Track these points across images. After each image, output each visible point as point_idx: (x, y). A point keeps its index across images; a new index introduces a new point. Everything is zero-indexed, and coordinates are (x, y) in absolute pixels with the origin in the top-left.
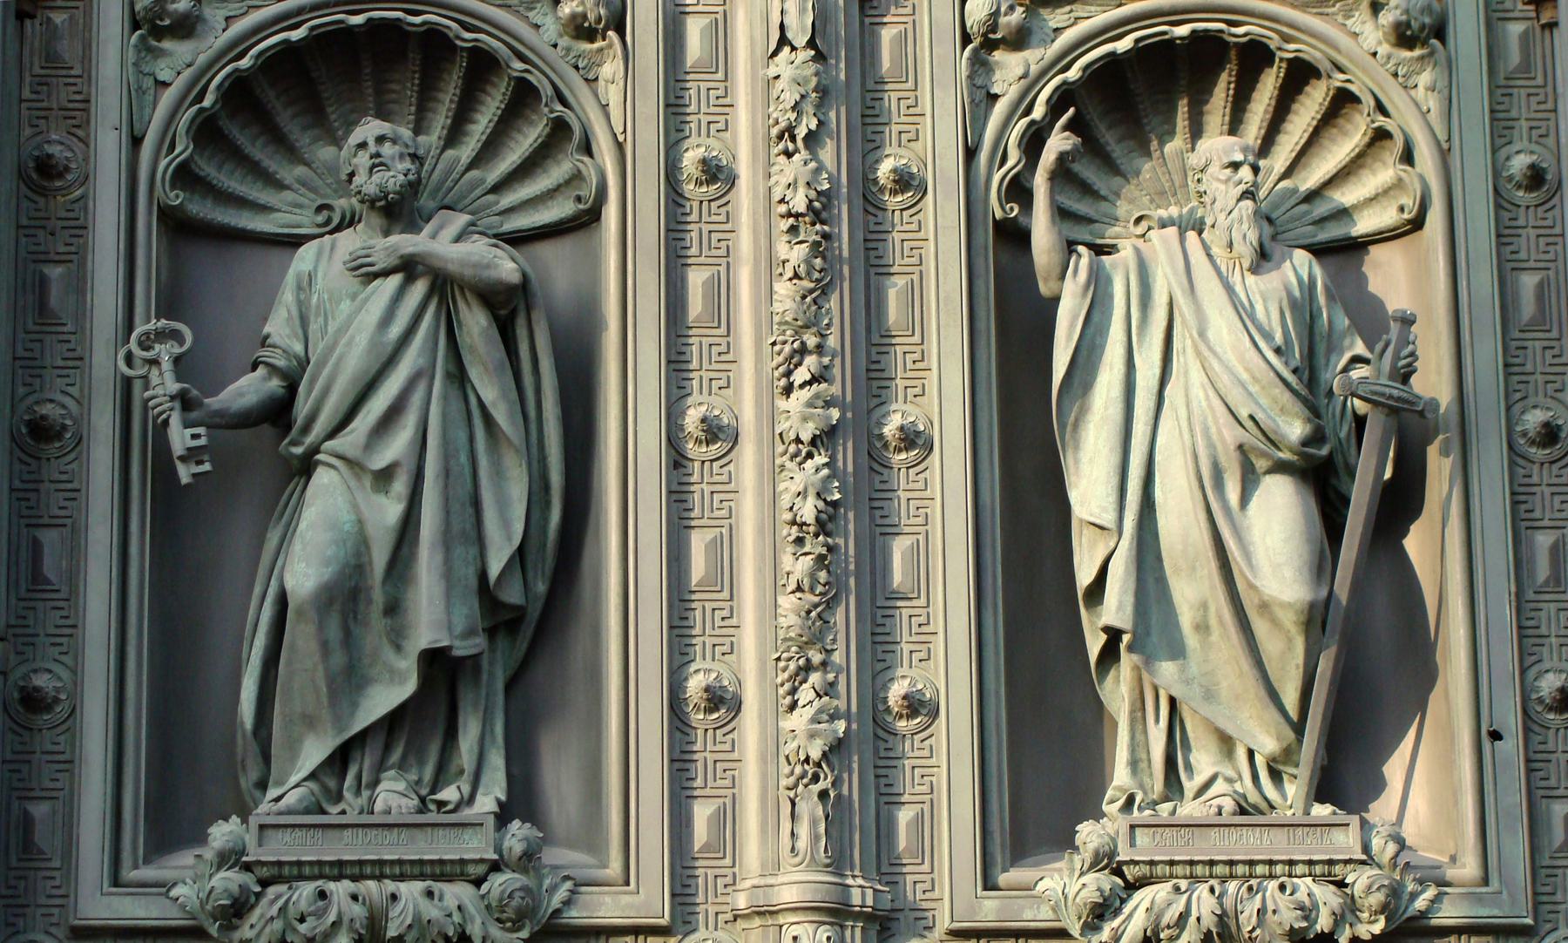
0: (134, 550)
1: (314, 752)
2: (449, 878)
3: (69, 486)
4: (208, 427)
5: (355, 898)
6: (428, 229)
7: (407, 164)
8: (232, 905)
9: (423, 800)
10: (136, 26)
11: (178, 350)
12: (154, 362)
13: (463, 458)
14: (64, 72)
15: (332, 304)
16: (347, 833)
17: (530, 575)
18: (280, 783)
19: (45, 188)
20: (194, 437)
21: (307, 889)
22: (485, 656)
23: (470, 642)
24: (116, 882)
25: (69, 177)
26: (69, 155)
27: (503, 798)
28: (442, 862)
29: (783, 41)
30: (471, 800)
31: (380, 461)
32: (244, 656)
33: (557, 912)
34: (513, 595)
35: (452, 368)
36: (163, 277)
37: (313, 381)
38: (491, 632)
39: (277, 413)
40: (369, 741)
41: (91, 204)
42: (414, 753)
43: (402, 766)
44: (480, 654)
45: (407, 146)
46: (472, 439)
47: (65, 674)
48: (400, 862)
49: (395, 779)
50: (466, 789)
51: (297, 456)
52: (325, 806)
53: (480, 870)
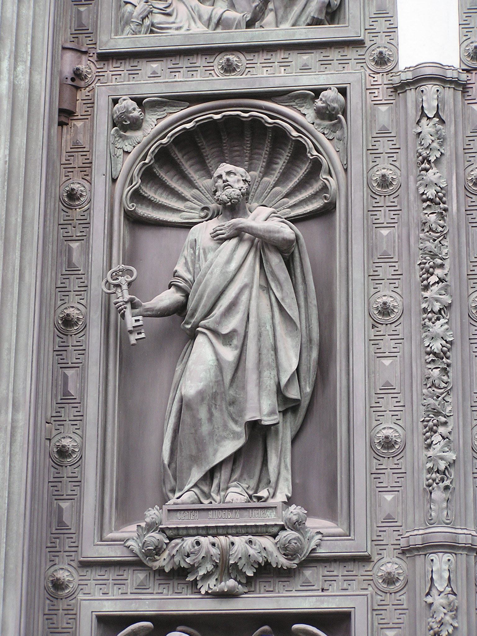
0: (111, 377)
1: (196, 475)
2: (261, 535)
3: (81, 348)
4: (144, 316)
5: (213, 545)
6: (252, 215)
7: (241, 184)
8: (155, 549)
9: (250, 497)
10: (114, 125)
11: (130, 279)
12: (118, 286)
13: (269, 327)
14: (81, 150)
15: (207, 256)
16: (210, 513)
17: (303, 383)
18: (181, 490)
19: (71, 205)
20: (136, 321)
21: (189, 541)
22: (280, 425)
23: (272, 418)
24: (101, 541)
25: (82, 199)
26: (82, 188)
27: (290, 495)
28: (256, 526)
29: (423, 114)
30: (274, 496)
31: (225, 330)
32: (165, 428)
33: (314, 550)
34: (293, 393)
35: (263, 283)
36: (127, 246)
37: (196, 291)
38: (284, 413)
39: (180, 310)
40: (223, 468)
41: (92, 211)
42: (247, 472)
43: (238, 480)
44: (278, 423)
45: (242, 176)
46: (273, 317)
47: (78, 439)
48: (236, 527)
49: (236, 486)
50: (272, 491)
51: (188, 329)
52: (203, 500)
53: (275, 530)
